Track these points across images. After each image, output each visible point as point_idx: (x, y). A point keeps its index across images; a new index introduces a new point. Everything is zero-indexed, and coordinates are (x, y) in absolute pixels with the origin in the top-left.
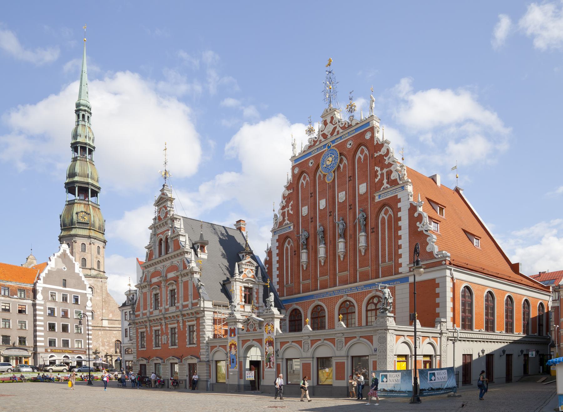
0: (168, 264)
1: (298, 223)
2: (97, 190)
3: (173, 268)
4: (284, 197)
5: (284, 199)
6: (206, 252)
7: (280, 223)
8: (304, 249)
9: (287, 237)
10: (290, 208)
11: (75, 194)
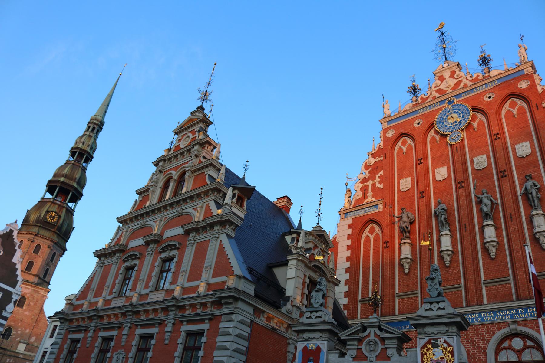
0: (171, 213)
1: (393, 201)
2: (78, 196)
4: (367, 167)
5: (366, 169)
6: (245, 208)
7: (357, 201)
9: (372, 221)
10: (378, 179)
11: (52, 195)
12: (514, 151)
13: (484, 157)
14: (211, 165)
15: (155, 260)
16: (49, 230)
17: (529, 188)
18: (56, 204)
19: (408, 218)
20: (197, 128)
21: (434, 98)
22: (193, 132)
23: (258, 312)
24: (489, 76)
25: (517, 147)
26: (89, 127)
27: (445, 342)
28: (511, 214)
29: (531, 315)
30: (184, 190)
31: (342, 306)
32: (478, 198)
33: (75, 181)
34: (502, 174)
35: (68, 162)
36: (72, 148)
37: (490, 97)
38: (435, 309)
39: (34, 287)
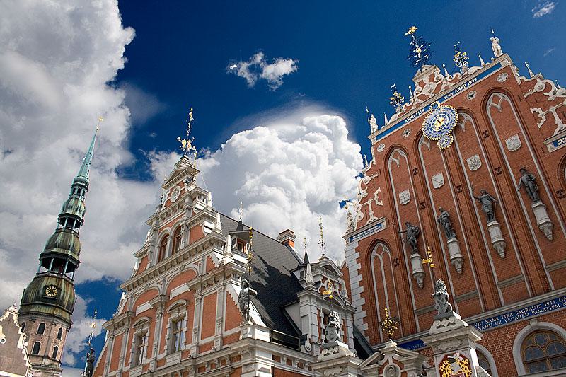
0: (174, 272)
1: (395, 216)
3: (185, 276)
8: (416, 252)
10: (376, 197)
12: (505, 146)
13: (477, 156)
14: (204, 216)
15: (165, 323)
16: (48, 305)
17: (525, 181)
18: (53, 277)
19: (413, 231)
20: (184, 179)
21: (418, 105)
22: (181, 185)
23: (276, 358)
24: (467, 74)
25: (507, 142)
26: (74, 190)
27: (461, 355)
28: (513, 211)
29: (549, 309)
30: (182, 246)
31: (363, 333)
32: (478, 199)
33: (69, 249)
34: (497, 172)
35: (58, 231)
36: (60, 216)
37: (472, 96)
38: (446, 325)
39: (45, 369)
